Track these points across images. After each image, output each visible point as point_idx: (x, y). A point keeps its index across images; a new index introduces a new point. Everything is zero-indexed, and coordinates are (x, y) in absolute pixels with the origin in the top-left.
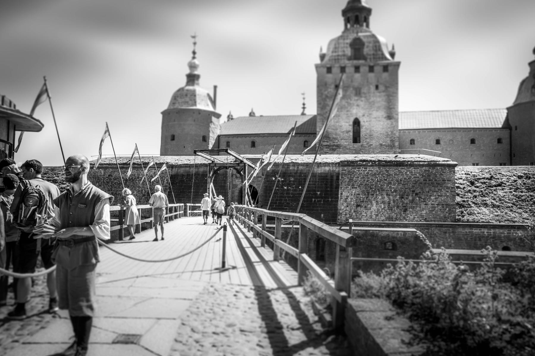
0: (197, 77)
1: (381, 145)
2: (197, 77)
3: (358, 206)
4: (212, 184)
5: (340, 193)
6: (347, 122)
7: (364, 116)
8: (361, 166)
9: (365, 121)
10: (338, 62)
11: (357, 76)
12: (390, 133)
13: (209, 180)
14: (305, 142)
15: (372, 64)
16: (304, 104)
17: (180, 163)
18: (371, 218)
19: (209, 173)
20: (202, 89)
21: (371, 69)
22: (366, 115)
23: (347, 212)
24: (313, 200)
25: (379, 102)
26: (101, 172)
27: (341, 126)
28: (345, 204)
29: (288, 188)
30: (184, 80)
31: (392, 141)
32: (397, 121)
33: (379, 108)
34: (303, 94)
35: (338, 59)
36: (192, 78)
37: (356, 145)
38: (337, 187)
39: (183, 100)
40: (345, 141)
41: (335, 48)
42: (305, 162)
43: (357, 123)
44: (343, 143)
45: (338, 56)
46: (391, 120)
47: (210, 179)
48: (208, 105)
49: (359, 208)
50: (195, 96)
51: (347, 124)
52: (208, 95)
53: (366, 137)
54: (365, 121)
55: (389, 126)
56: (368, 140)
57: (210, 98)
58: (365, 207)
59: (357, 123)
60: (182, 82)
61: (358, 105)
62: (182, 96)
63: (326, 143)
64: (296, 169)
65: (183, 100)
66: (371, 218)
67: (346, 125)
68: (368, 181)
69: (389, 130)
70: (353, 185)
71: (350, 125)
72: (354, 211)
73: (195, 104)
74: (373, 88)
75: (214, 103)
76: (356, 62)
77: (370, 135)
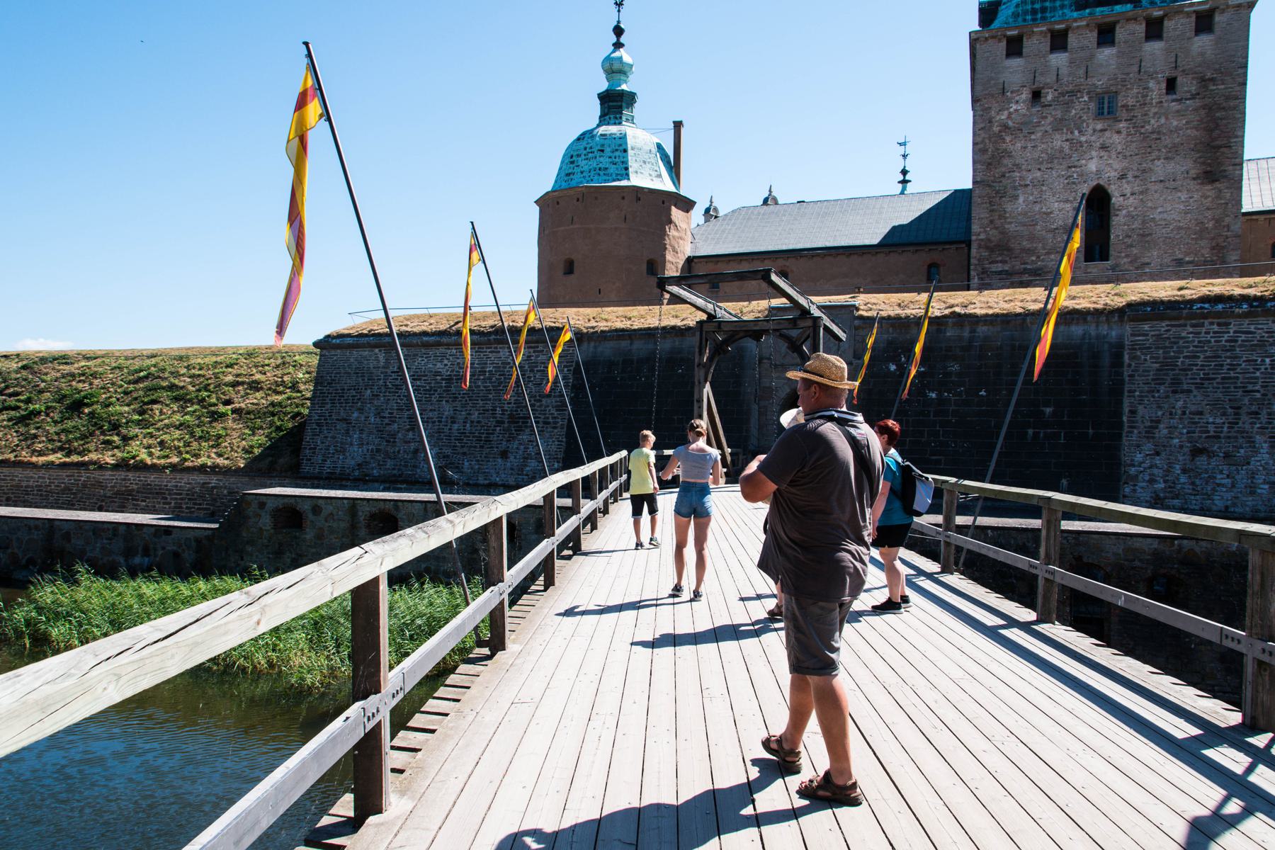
0: (630, 99)
2: (630, 99)
3: (1196, 452)
4: (707, 389)
5: (1126, 410)
6: (1067, 201)
7: (1122, 177)
8: (1205, 317)
9: (1128, 192)
10: (1043, 18)
11: (1107, 53)
13: (699, 374)
14: (930, 266)
15: (1157, 13)
16: (904, 172)
17: (603, 326)
18: (1253, 493)
19: (701, 354)
20: (641, 134)
21: (1154, 30)
23: (1155, 471)
24: (1030, 431)
25: (1178, 129)
26: (377, 359)
28: (1148, 447)
29: (940, 394)
30: (595, 108)
32: (1236, 185)
33: (1174, 149)
34: (903, 144)
36: (615, 103)
38: (1117, 391)
39: (594, 164)
42: (997, 311)
46: (1217, 185)
47: (702, 373)
48: (660, 176)
49: (1202, 461)
50: (625, 151)
52: (659, 147)
53: (1129, 241)
54: (1128, 192)
55: (1207, 202)
56: (1135, 251)
57: (664, 157)
58: (1227, 456)
60: (589, 114)
61: (1104, 147)
62: (589, 152)
63: (999, 267)
64: (966, 334)
65: (594, 164)
66: (1253, 493)
68: (1233, 367)
69: (1209, 214)
70: (1176, 382)
72: (1184, 471)
73: (627, 176)
74: (1156, 88)
75: (674, 169)
77: (1143, 235)
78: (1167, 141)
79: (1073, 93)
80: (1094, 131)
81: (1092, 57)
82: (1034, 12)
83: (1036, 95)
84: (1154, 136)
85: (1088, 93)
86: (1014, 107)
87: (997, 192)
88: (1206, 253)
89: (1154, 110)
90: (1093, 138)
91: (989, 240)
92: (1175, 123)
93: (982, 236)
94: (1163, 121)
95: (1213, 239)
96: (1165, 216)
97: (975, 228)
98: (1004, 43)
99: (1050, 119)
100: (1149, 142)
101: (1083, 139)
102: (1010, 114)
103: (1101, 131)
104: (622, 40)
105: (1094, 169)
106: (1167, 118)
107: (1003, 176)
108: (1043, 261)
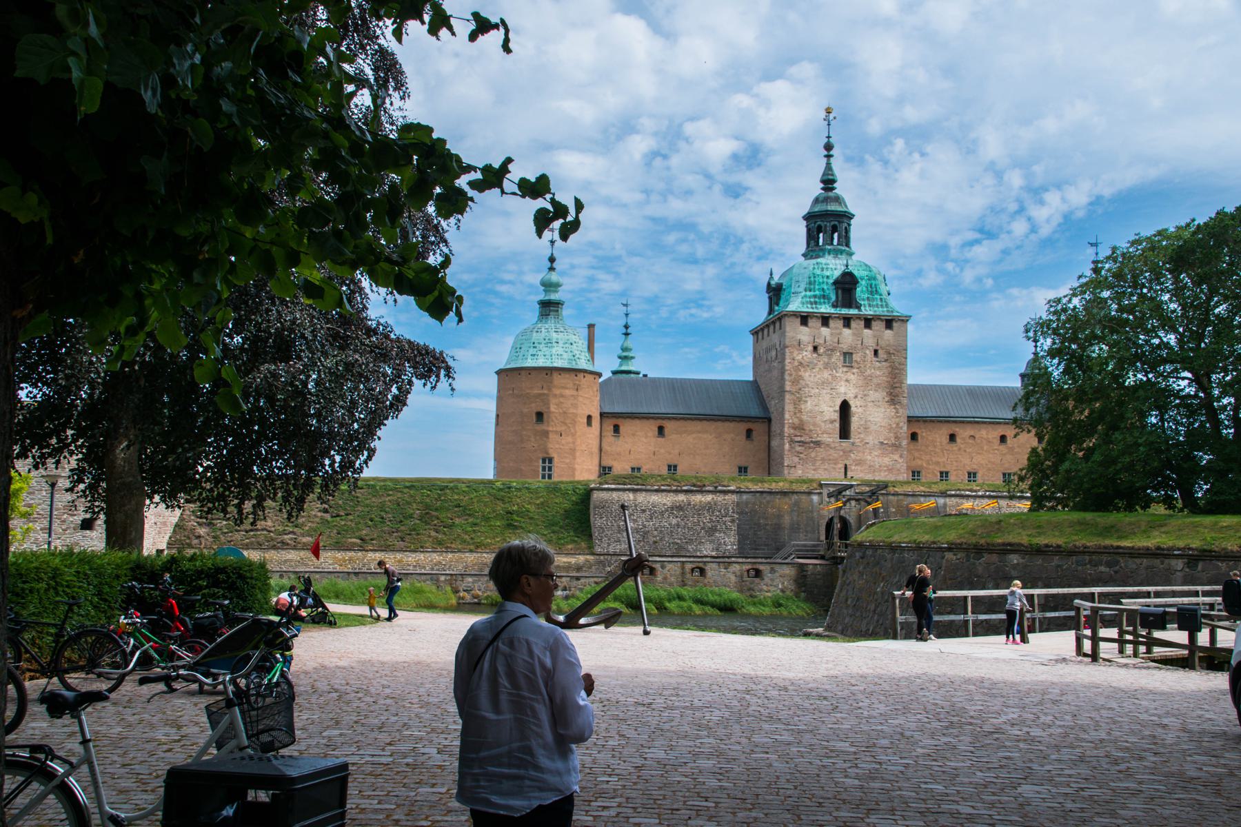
11: (846, 331)
16: (626, 327)
37: (845, 444)
41: (810, 283)
43: (845, 408)
44: (825, 438)
67: (830, 412)
74: (870, 353)
76: (844, 311)
78: (875, 381)
79: (832, 350)
83: (815, 348)
97: (787, 416)
98: (799, 320)
104: (555, 265)
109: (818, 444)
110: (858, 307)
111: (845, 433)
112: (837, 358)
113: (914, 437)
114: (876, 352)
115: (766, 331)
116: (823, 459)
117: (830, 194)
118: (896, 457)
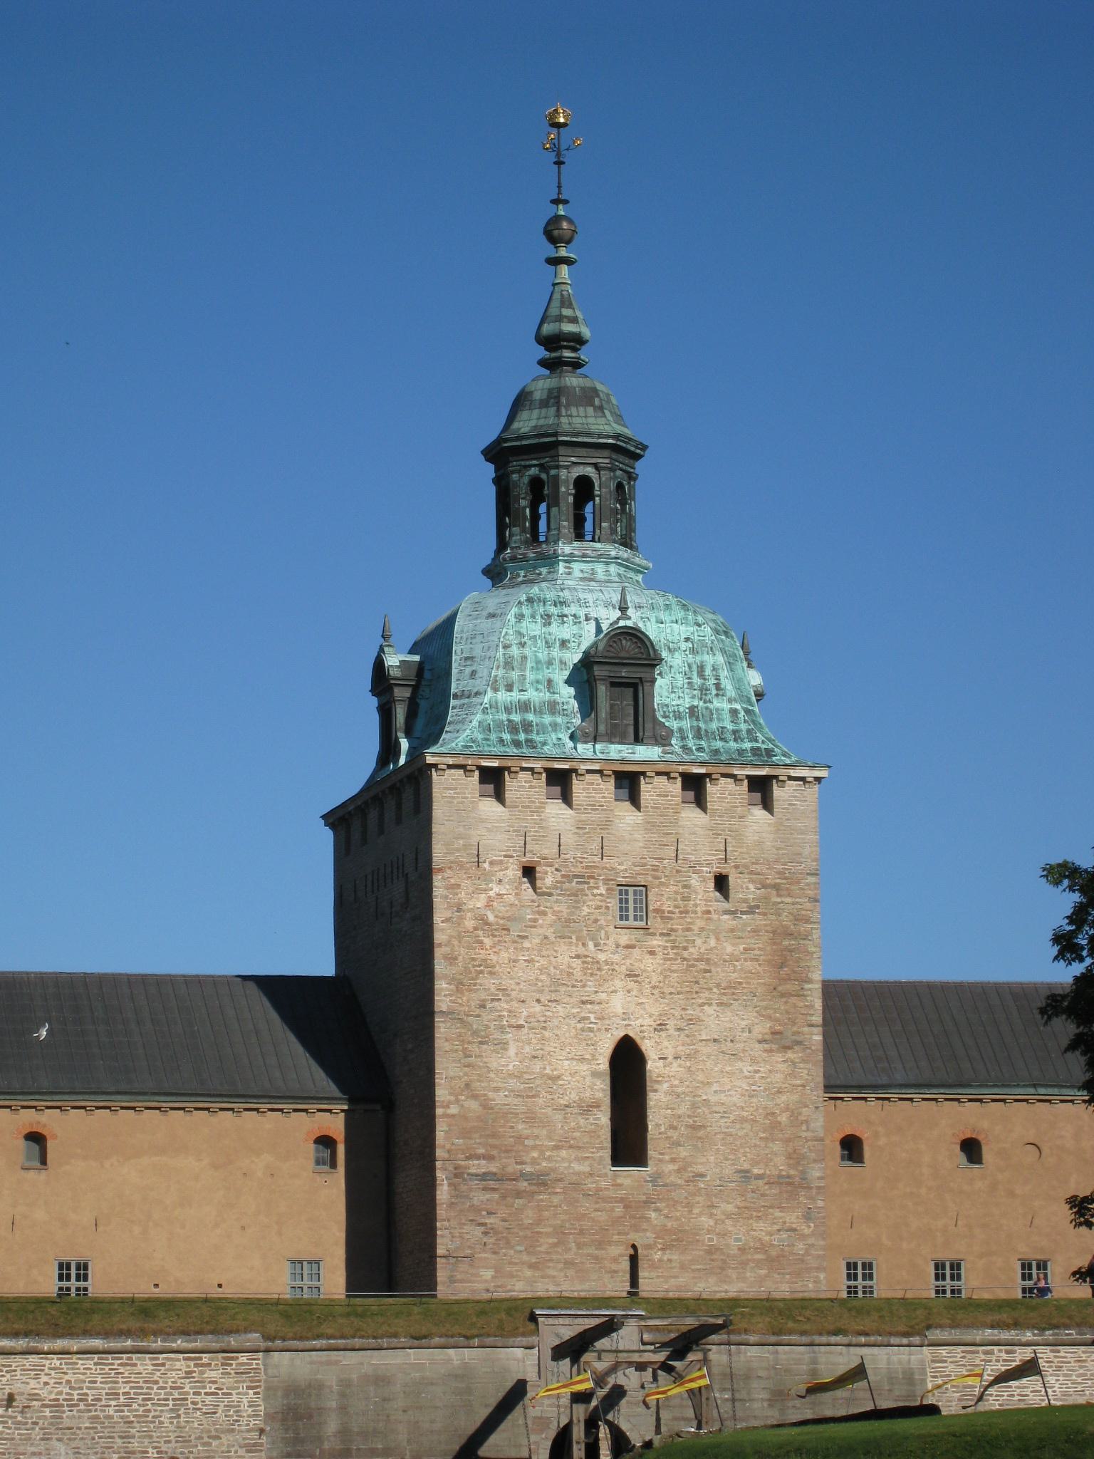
1: (745, 1175)
6: (582, 1060)
7: (661, 1027)
9: (670, 1053)
12: (783, 1118)
22: (671, 1024)
27: (555, 1079)
31: (795, 1158)
35: (527, 727)
37: (629, 1175)
40: (573, 1154)
44: (569, 1164)
45: (525, 707)
46: (790, 1054)
51: (584, 1068)
53: (674, 1135)
54: (670, 1053)
59: (627, 1064)
61: (632, 975)
71: (595, 1074)
74: (703, 889)
76: (617, 751)
77: (694, 1128)
80: (618, 946)
81: (606, 824)
82: (513, 728)
83: (529, 872)
84: (702, 965)
85: (606, 881)
86: (496, 889)
87: (475, 1033)
88: (780, 1165)
89: (700, 923)
90: (616, 958)
91: (465, 1118)
92: (729, 949)
93: (453, 1110)
94: (712, 942)
95: (789, 1140)
96: (722, 1097)
99: (550, 917)
100: (695, 975)
101: (602, 957)
102: (490, 899)
103: (628, 947)
105: (620, 1011)
106: (718, 939)
107: (483, 1006)
108: (549, 1159)
109: (541, 1181)
110: (662, 739)
111: (628, 1143)
112: (598, 902)
113: (852, 1148)
114: (721, 883)
115: (373, 815)
116: (560, 1232)
117: (572, 380)
118: (792, 1218)
